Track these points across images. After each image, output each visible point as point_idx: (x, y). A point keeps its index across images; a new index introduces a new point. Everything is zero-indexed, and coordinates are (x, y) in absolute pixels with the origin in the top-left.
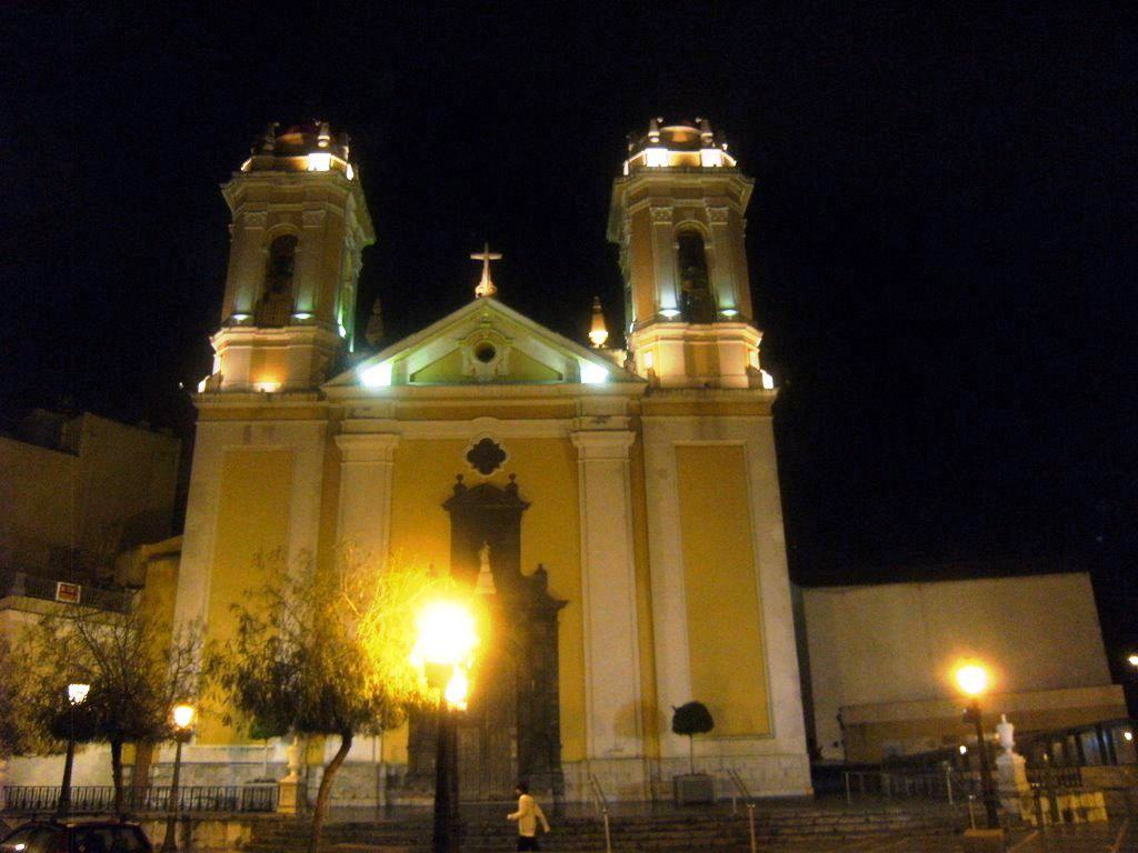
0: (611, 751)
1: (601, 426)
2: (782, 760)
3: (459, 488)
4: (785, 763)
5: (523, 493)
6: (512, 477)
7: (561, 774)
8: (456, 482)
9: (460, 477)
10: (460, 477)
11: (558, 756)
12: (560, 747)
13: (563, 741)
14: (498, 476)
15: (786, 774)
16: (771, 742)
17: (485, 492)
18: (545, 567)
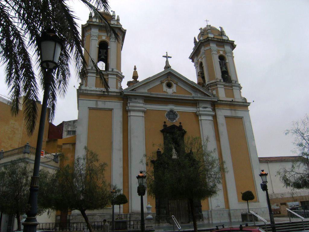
0: (216, 207)
1: (205, 109)
2: (262, 209)
3: (165, 126)
4: (263, 210)
5: (184, 128)
6: (180, 123)
7: (203, 215)
8: (164, 124)
9: (165, 122)
10: (165, 122)
11: (201, 209)
12: (201, 206)
14: (176, 122)
15: (263, 212)
16: (257, 204)
17: (174, 127)
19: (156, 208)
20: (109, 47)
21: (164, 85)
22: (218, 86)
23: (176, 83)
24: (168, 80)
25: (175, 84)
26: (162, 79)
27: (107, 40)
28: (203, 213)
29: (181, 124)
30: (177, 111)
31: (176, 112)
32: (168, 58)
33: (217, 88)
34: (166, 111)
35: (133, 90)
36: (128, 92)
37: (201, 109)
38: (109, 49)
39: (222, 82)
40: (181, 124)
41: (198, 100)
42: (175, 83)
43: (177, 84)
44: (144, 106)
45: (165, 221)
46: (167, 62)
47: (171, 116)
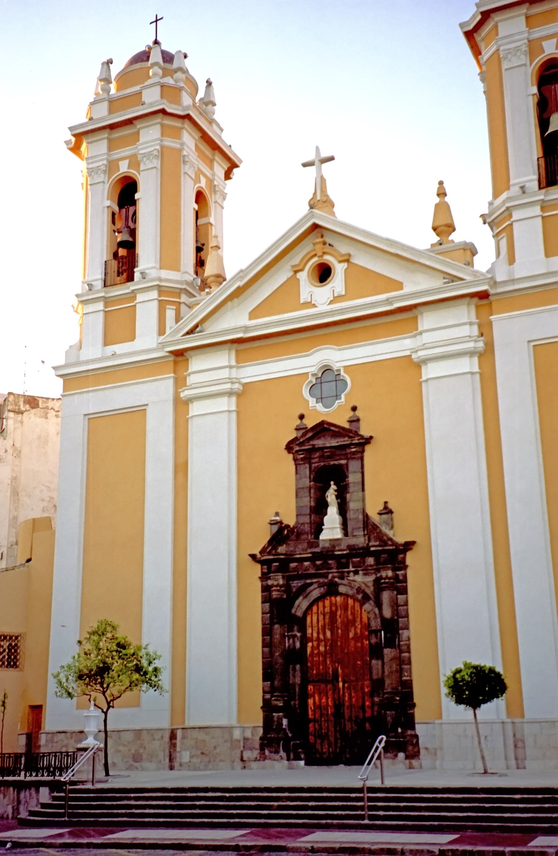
7: (417, 736)
12: (414, 706)
13: (417, 699)
18: (390, 506)
19: (264, 711)
20: (137, 196)
21: (303, 276)
22: (516, 215)
23: (346, 258)
24: (315, 255)
25: (340, 262)
26: (296, 258)
27: (133, 173)
28: (420, 729)
29: (358, 413)
30: (345, 367)
31: (339, 370)
32: (324, 165)
33: (511, 225)
34: (307, 373)
35: (191, 332)
36: (178, 342)
37: (427, 338)
38: (138, 199)
39: (534, 194)
40: (358, 413)
41: (415, 306)
42: (341, 259)
43: (348, 261)
44: (234, 373)
45: (282, 754)
46: (322, 182)
47: (329, 388)
